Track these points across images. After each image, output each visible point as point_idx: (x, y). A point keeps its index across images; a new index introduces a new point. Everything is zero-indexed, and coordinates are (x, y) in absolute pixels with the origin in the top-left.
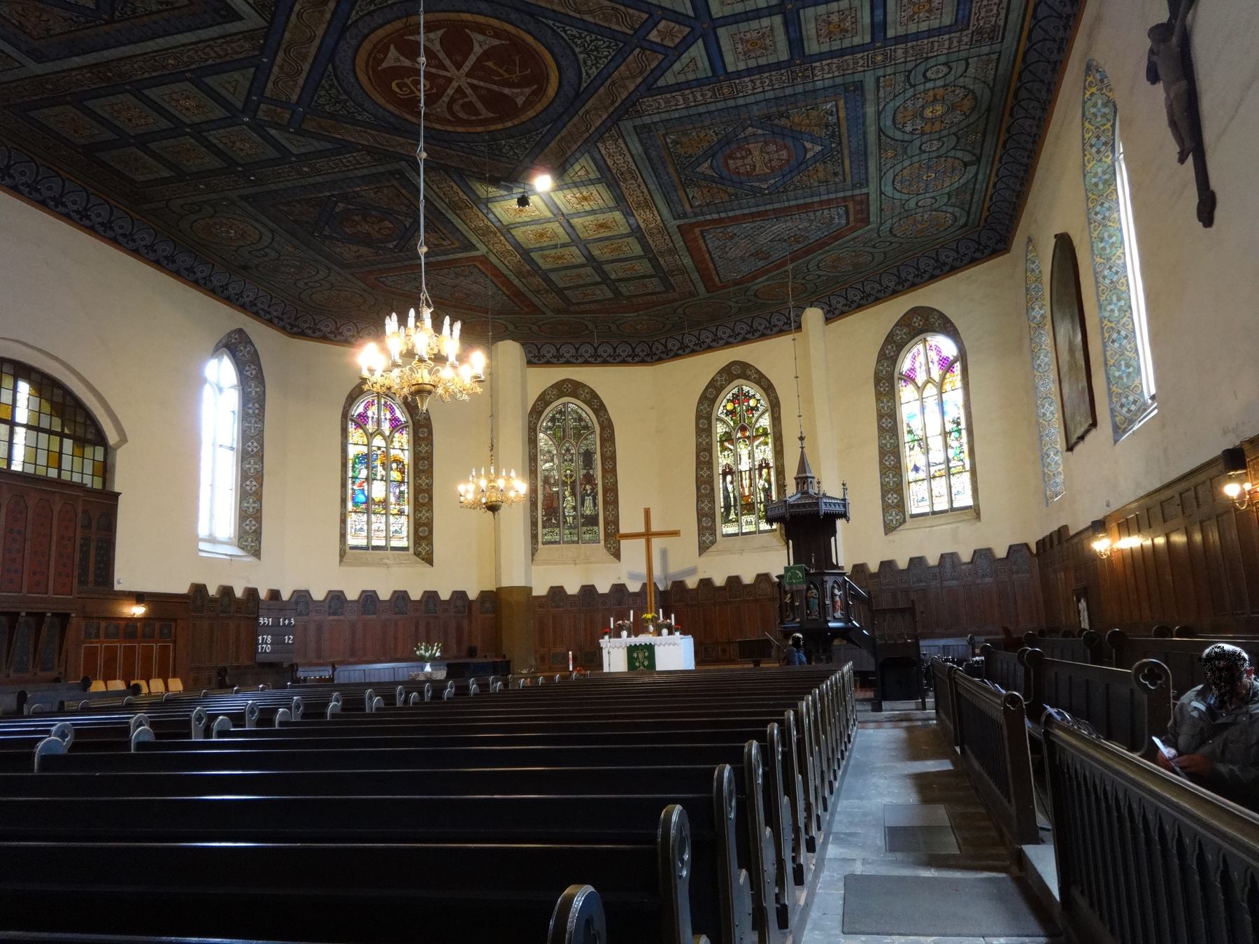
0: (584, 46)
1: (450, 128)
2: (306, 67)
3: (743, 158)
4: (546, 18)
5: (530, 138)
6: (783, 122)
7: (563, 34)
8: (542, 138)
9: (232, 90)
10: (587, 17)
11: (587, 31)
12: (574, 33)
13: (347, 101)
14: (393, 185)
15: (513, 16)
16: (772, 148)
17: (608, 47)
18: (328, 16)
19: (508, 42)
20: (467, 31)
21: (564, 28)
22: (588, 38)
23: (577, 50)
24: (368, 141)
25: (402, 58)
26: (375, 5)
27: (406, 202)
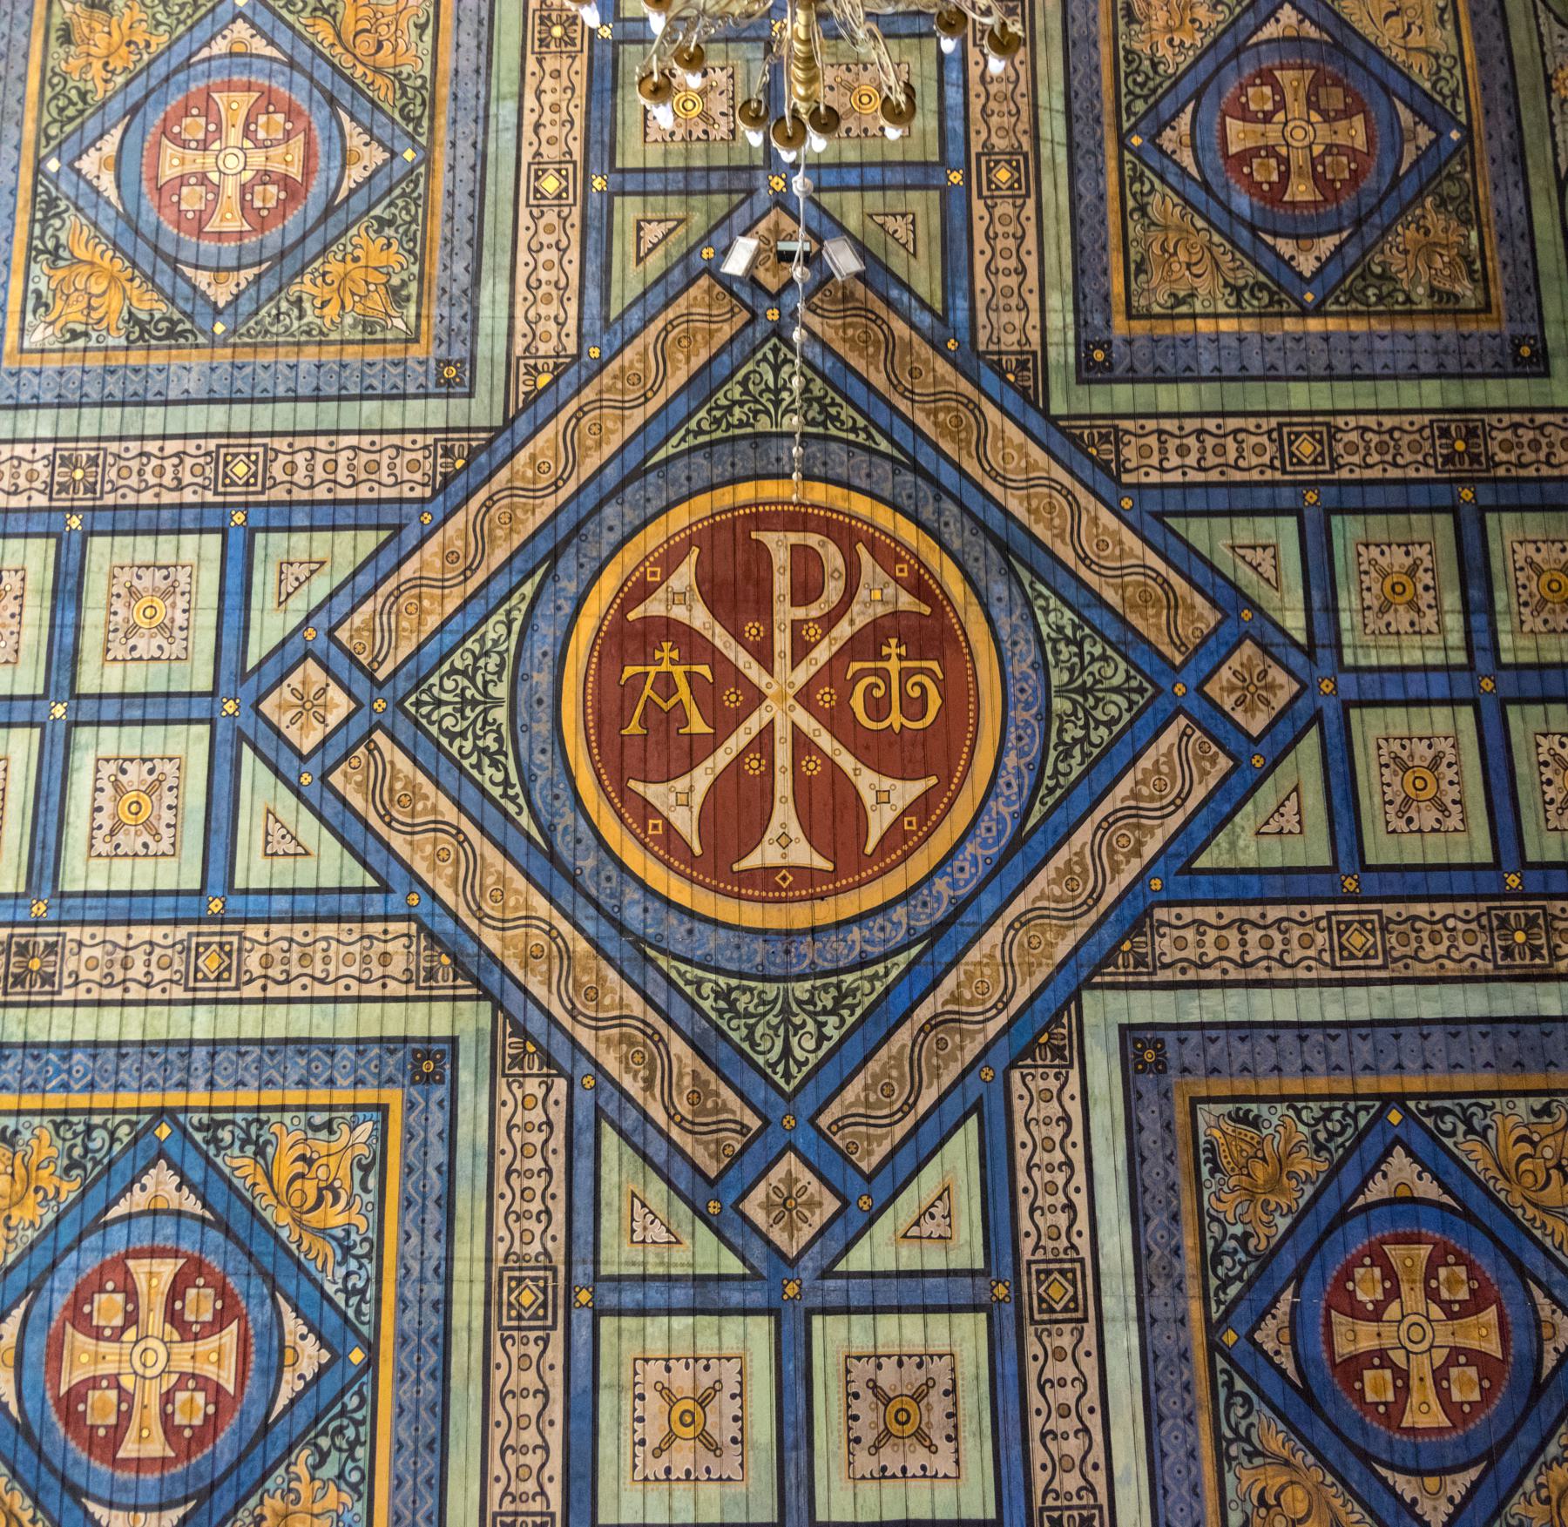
0: (485, 722)
1: (884, 517)
2: (1083, 835)
3: (264, 177)
4: (529, 837)
5: (717, 421)
6: (148, 304)
7: (514, 778)
8: (690, 416)
9: (1291, 806)
10: (449, 812)
11: (461, 768)
12: (489, 771)
13: (1063, 691)
14: (1130, 316)
15: (588, 864)
16: (192, 199)
17: (439, 703)
18: (949, 983)
19: (632, 784)
20: (697, 850)
21: (505, 795)
22: (468, 746)
23: (500, 714)
24: (1095, 520)
25: (869, 798)
26: (838, 986)
27: (1135, 230)
